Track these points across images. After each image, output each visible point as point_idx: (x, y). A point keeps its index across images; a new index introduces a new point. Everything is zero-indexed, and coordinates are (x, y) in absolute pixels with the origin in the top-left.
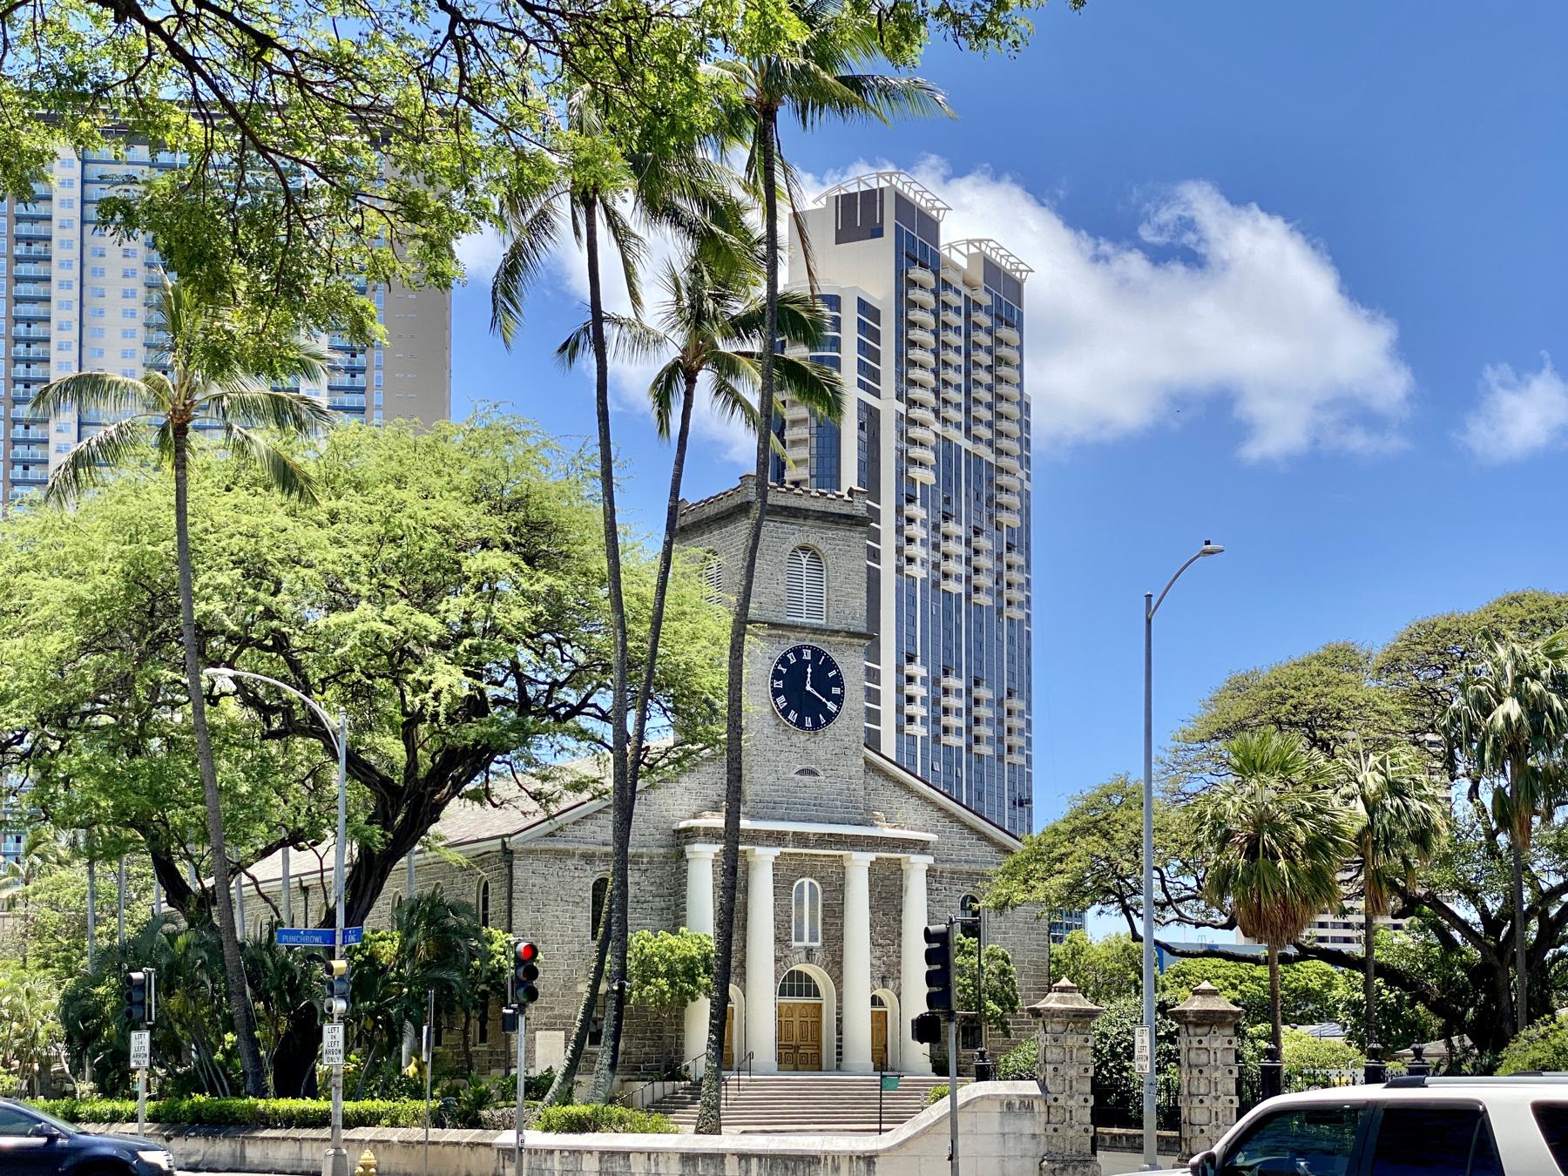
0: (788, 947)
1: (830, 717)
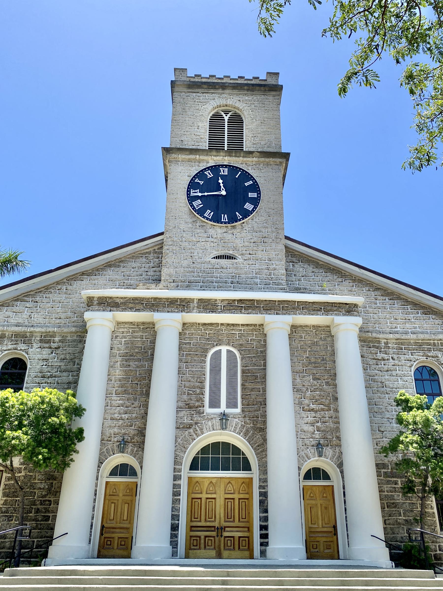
0: (200, 413)
1: (246, 214)
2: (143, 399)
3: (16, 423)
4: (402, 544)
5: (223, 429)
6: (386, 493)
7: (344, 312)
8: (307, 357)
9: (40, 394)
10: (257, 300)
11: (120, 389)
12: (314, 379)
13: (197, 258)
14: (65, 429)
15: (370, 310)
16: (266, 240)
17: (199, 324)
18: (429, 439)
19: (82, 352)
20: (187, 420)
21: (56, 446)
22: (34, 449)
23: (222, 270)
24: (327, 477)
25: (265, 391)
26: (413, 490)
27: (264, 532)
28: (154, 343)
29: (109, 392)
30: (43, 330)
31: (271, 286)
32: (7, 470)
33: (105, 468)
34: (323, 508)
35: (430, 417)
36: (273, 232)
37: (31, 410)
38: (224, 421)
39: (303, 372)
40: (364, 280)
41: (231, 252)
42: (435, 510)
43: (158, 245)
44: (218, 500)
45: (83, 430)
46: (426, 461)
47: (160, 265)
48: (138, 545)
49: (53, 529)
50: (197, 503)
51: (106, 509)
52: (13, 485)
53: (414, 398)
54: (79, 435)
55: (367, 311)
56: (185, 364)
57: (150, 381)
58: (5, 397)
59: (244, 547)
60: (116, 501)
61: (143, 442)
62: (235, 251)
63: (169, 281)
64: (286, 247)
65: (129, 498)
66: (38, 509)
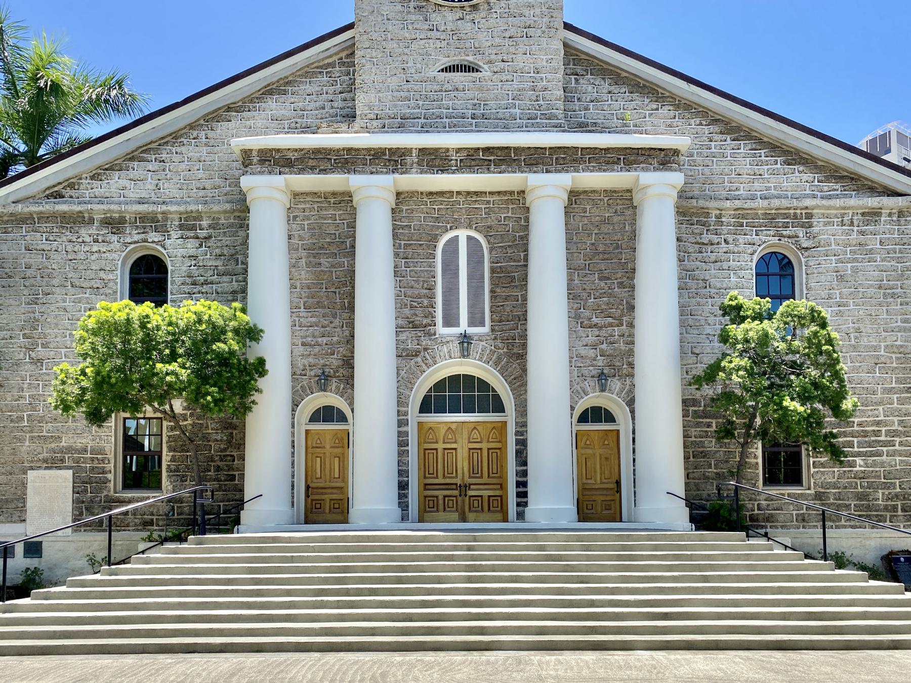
2: (345, 315)
3: (167, 351)
4: (708, 503)
5: (464, 356)
6: (693, 439)
7: (656, 165)
8: (593, 244)
9: (193, 309)
10: (514, 148)
11: (310, 300)
12: (600, 279)
13: (413, 71)
14: (239, 360)
15: (699, 160)
16: (531, 32)
17: (422, 193)
18: (765, 363)
19: (245, 243)
20: (411, 346)
21: (228, 384)
22: (198, 388)
23: (456, 93)
24: (610, 418)
25: (526, 300)
26: (733, 435)
27: (521, 489)
28: (354, 227)
29: (294, 304)
30: (182, 208)
31: (539, 120)
32: (167, 417)
33: (302, 412)
34: (603, 459)
35: (771, 331)
36: (543, 15)
37: (184, 332)
38: (465, 345)
39: (584, 269)
40: (694, 106)
41: (471, 58)
42: (760, 460)
43: (347, 48)
44: (459, 451)
45: (265, 361)
46: (755, 394)
47: (351, 88)
48: (356, 507)
49: (242, 491)
50: (431, 455)
51: (310, 464)
52: (179, 436)
53: (750, 301)
54: (260, 367)
55: (694, 161)
56: (403, 261)
57: (353, 287)
58: (144, 314)
59: (496, 508)
60: (321, 455)
61: (352, 377)
62: (478, 56)
63: (369, 116)
64: (565, 45)
65: (340, 450)
66: (219, 467)
